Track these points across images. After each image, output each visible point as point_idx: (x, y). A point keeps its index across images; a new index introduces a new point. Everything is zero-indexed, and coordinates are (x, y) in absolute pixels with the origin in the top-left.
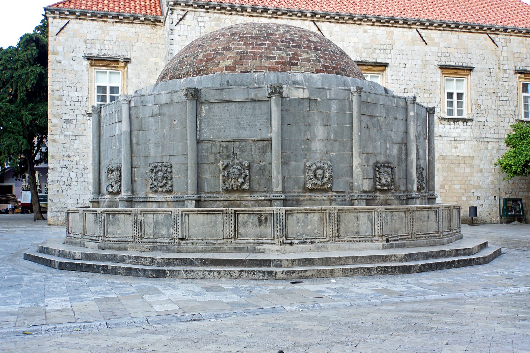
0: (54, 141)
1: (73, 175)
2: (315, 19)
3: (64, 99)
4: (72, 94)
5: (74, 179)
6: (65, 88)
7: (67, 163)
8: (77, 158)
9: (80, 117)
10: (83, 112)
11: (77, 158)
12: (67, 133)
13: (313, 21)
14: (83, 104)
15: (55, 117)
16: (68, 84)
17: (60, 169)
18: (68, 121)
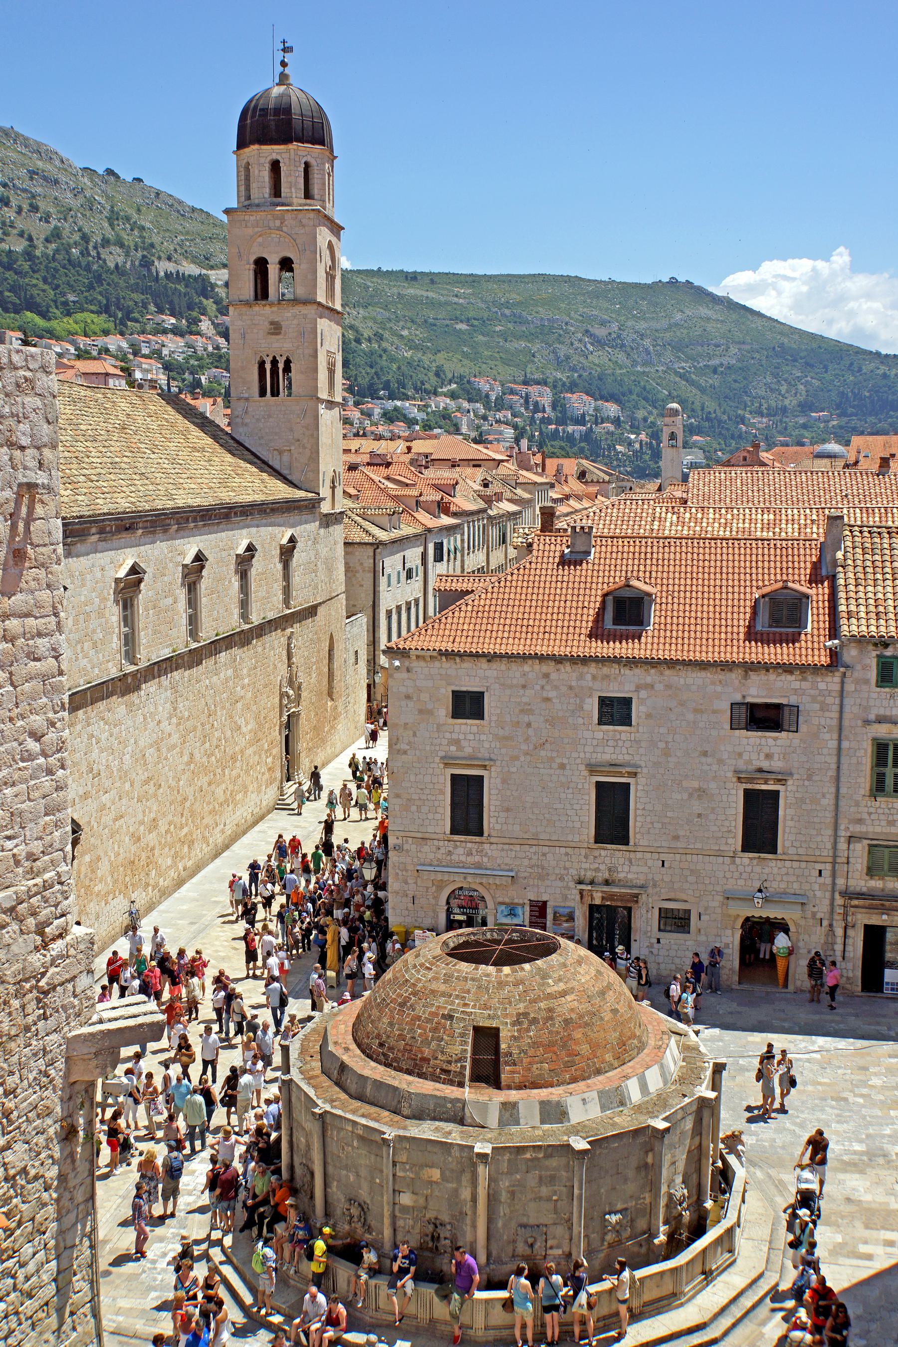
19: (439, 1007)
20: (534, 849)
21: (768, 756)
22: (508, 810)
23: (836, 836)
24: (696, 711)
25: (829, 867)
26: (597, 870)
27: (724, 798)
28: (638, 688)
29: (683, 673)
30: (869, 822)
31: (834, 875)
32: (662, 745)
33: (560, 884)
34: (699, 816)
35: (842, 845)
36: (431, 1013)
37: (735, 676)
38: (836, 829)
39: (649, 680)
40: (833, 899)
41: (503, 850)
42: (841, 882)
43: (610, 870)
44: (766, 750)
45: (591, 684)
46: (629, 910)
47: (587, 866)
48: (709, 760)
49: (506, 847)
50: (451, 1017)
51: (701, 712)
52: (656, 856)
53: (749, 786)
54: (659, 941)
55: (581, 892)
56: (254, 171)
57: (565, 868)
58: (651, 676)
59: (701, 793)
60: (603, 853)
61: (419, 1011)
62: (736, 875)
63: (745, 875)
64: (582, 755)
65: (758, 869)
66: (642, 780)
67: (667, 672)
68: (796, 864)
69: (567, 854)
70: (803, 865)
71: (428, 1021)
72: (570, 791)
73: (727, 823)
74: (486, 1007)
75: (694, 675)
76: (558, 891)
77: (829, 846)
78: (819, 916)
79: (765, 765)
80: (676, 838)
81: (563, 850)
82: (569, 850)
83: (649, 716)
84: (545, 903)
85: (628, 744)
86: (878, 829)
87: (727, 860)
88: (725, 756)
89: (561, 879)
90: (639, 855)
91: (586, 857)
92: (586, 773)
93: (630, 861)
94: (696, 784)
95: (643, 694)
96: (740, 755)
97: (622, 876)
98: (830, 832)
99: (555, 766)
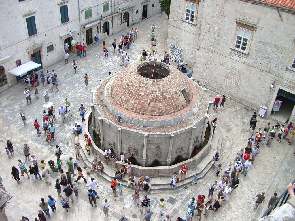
0: (170, 27)
1: (175, 42)
2: (279, 10)
3: (175, 12)
4: (178, 10)
5: (175, 44)
6: (176, 7)
7: (174, 37)
8: (177, 36)
9: (179, 21)
10: (181, 19)
11: (177, 36)
12: (175, 26)
13: (278, 11)
14: (181, 15)
15: (171, 18)
16: (177, 6)
17: (171, 38)
18: (175, 21)
19: (172, 92)
20: (13, 46)
22: (4, 38)
23: (79, 11)
25: (78, 20)
26: (31, 44)
30: (84, 6)
31: (80, 22)
33: (22, 53)
34: (52, 18)
35: (80, 13)
36: (172, 95)
38: (79, 10)
40: (80, 27)
41: (5, 50)
42: (81, 22)
43: (34, 43)
46: (39, 51)
47: (27, 44)
49: (6, 49)
50: (177, 93)
52: (43, 33)
53: (61, 6)
54: (48, 55)
55: (28, 53)
57: (23, 47)
59: (51, 12)
60: (31, 38)
61: (169, 96)
62: (61, 30)
64: (21, 12)
65: (65, 27)
66: (37, 14)
68: (72, 22)
69: (22, 43)
70: (74, 21)
71: (173, 97)
72: (20, 24)
73: (57, 18)
74: (179, 86)
76: (22, 55)
77: (78, 15)
78: (78, 33)
80: (47, 27)
81: (21, 43)
82: (23, 42)
84: (20, 60)
85: (32, 4)
86: (86, 7)
89: (23, 51)
90: (40, 35)
91: (27, 42)
92: (22, 17)
93: (38, 38)
94: (49, 10)
97: (36, 43)
98: (78, 11)
99: (14, 18)
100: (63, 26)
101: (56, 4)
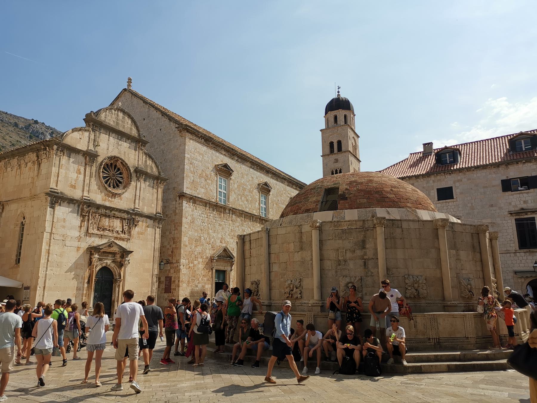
21: (525, 202)
24: (484, 187)
27: (505, 225)
28: (454, 182)
29: (475, 172)
32: (469, 205)
37: (502, 169)
39: (459, 178)
44: (524, 199)
45: (432, 184)
48: (494, 208)
51: (486, 187)
53: (517, 217)
56: (330, 119)
58: (460, 176)
63: (523, 261)
65: (530, 257)
67: (467, 173)
73: (509, 237)
75: (481, 172)
79: (524, 206)
83: (461, 193)
87: (512, 255)
88: (502, 205)
95: (457, 184)
96: (510, 204)
100: (523, 254)
101: (506, 213)
